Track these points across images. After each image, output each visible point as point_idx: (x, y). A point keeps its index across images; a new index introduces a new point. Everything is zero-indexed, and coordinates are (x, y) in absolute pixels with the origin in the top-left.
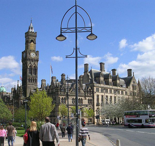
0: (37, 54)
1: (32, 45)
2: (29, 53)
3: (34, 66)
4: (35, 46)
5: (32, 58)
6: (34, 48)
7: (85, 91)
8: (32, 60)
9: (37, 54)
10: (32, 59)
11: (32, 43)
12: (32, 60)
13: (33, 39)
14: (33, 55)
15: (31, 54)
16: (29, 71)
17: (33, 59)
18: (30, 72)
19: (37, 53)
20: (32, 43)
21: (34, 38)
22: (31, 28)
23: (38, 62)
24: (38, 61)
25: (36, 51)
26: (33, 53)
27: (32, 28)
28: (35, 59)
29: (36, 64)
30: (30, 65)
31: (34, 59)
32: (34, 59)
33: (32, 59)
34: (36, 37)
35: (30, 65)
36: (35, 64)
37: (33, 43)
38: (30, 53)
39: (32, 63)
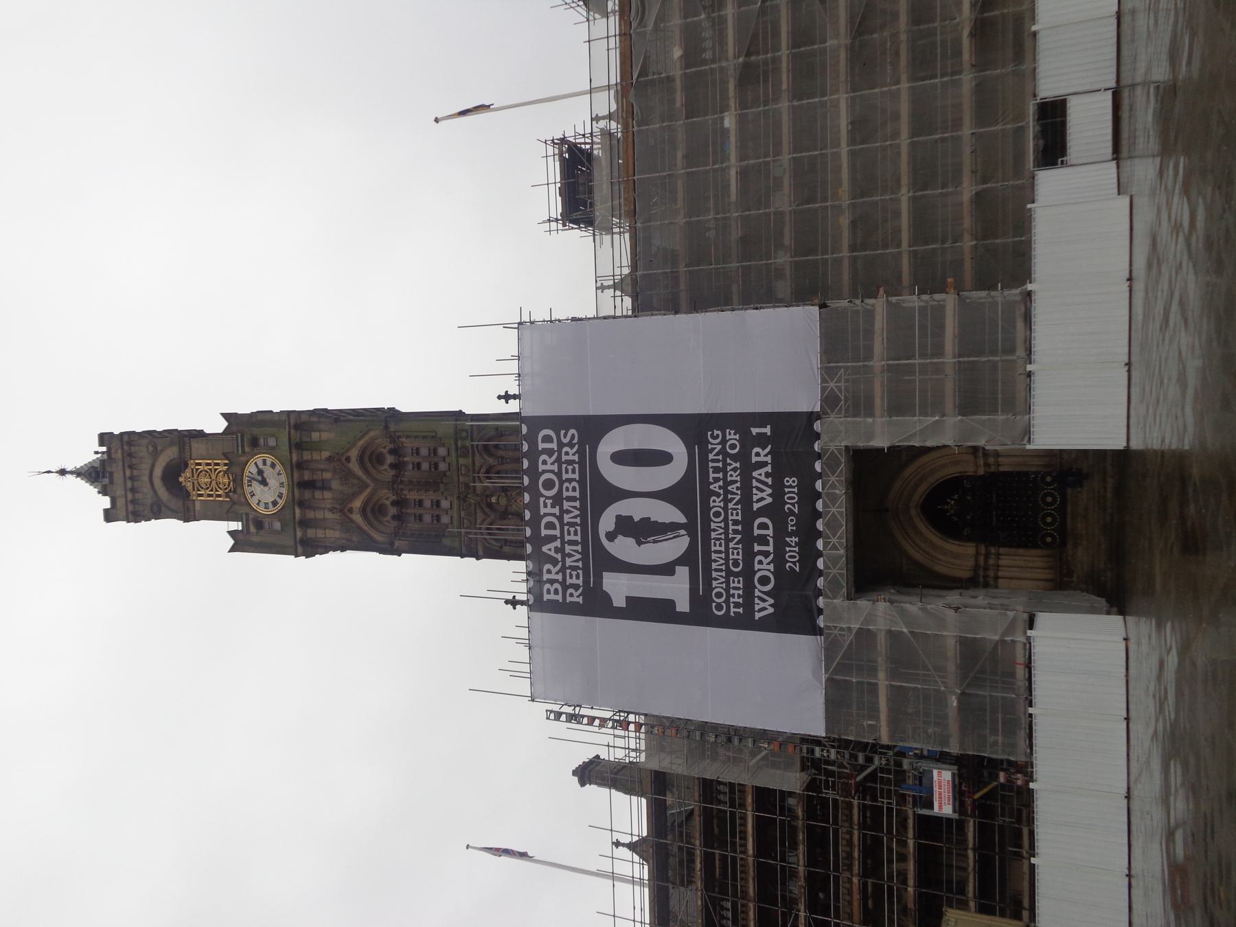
8: (304, 485)
11: (189, 486)
13: (158, 472)
15: (261, 510)
35: (357, 518)
37: (188, 473)
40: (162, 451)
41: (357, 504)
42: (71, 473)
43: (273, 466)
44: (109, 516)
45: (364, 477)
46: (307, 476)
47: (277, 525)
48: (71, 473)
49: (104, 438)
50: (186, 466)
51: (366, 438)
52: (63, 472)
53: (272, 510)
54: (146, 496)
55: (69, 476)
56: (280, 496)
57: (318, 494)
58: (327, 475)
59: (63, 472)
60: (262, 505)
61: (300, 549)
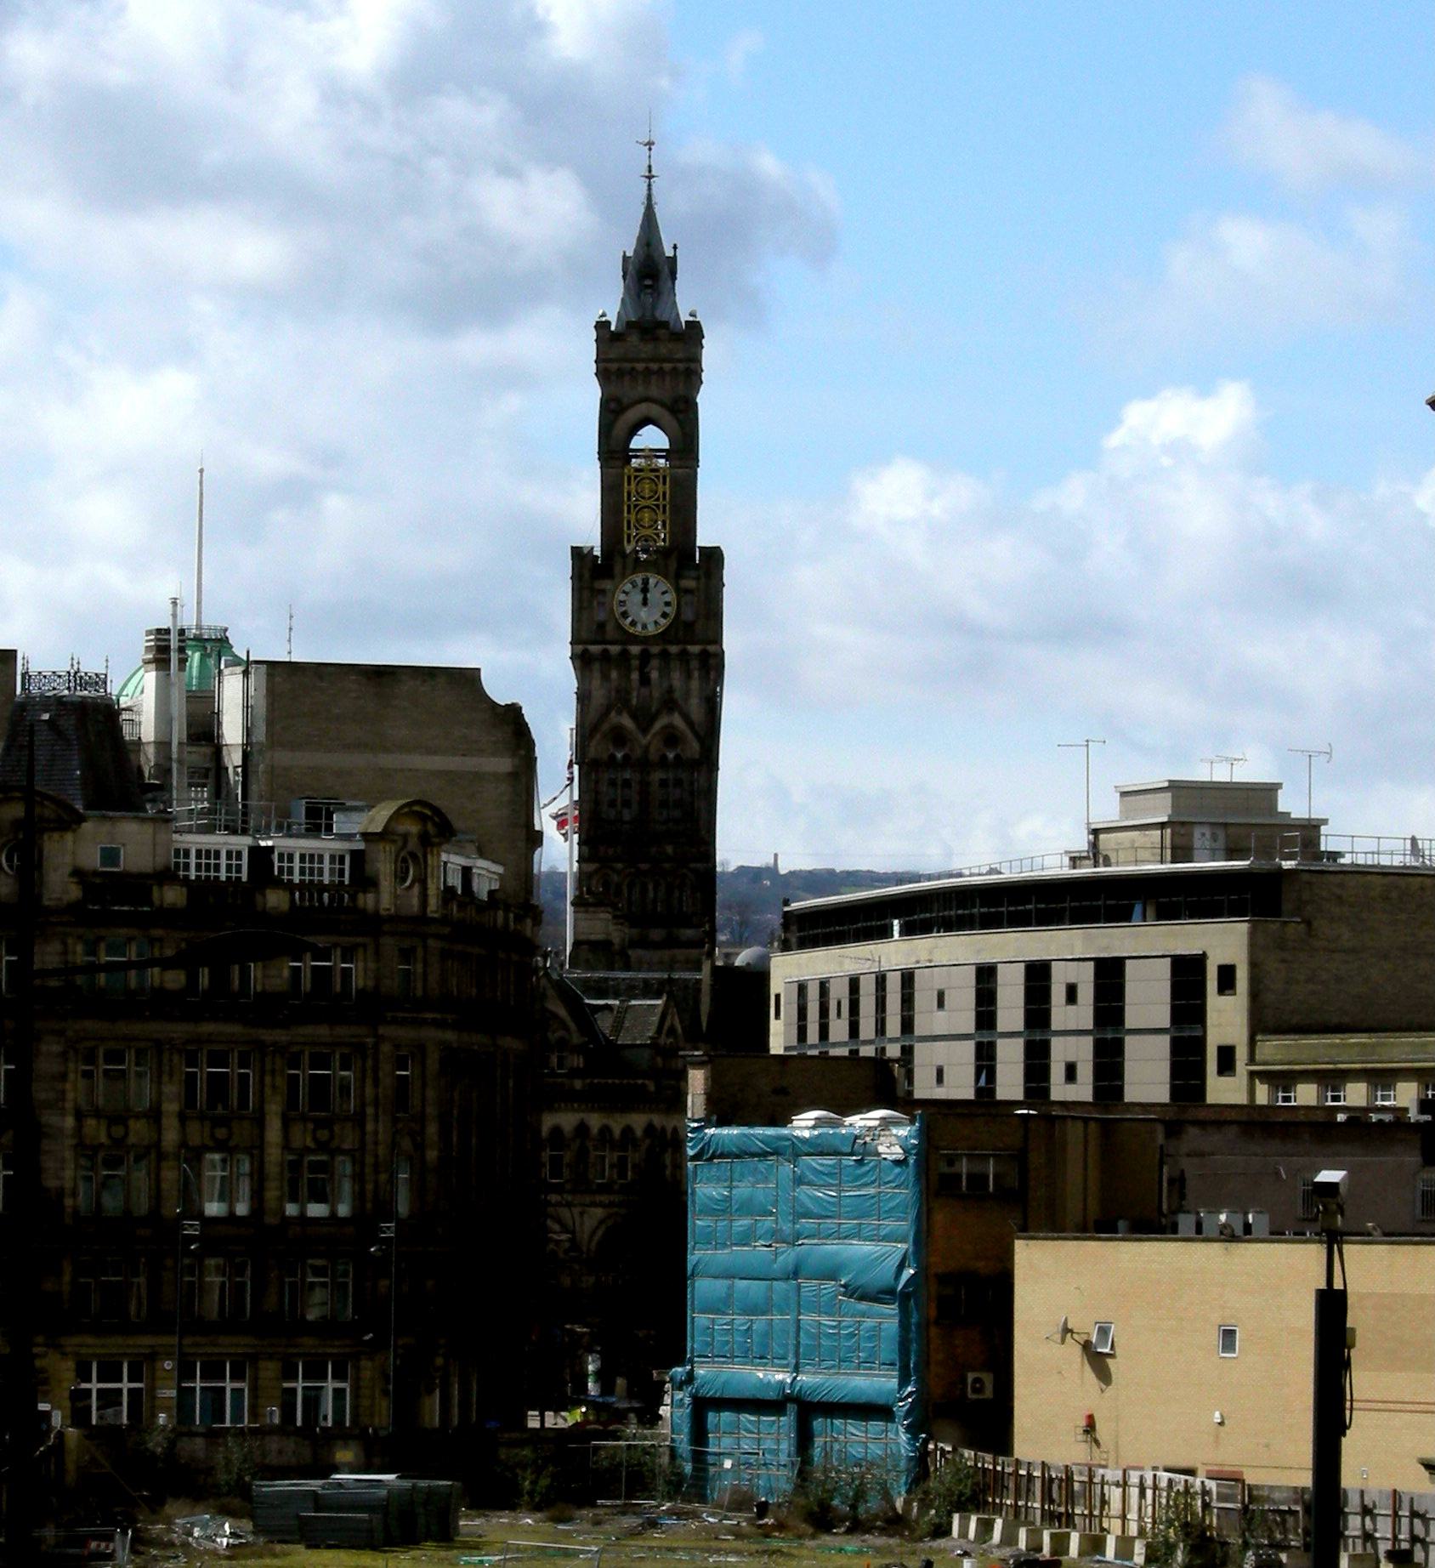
1: (647, 486)
3: (658, 726)
5: (635, 639)
12: (635, 663)
31: (655, 650)
32: (655, 650)
33: (635, 649)
40: (678, 420)
41: (627, 721)
42: (649, 197)
43: (664, 615)
44: (601, 326)
45: (653, 731)
46: (655, 663)
47: (601, 616)
48: (649, 197)
51: (690, 735)
53: (618, 610)
54: (629, 391)
57: (635, 676)
59: (650, 177)
60: (622, 597)
61: (580, 648)
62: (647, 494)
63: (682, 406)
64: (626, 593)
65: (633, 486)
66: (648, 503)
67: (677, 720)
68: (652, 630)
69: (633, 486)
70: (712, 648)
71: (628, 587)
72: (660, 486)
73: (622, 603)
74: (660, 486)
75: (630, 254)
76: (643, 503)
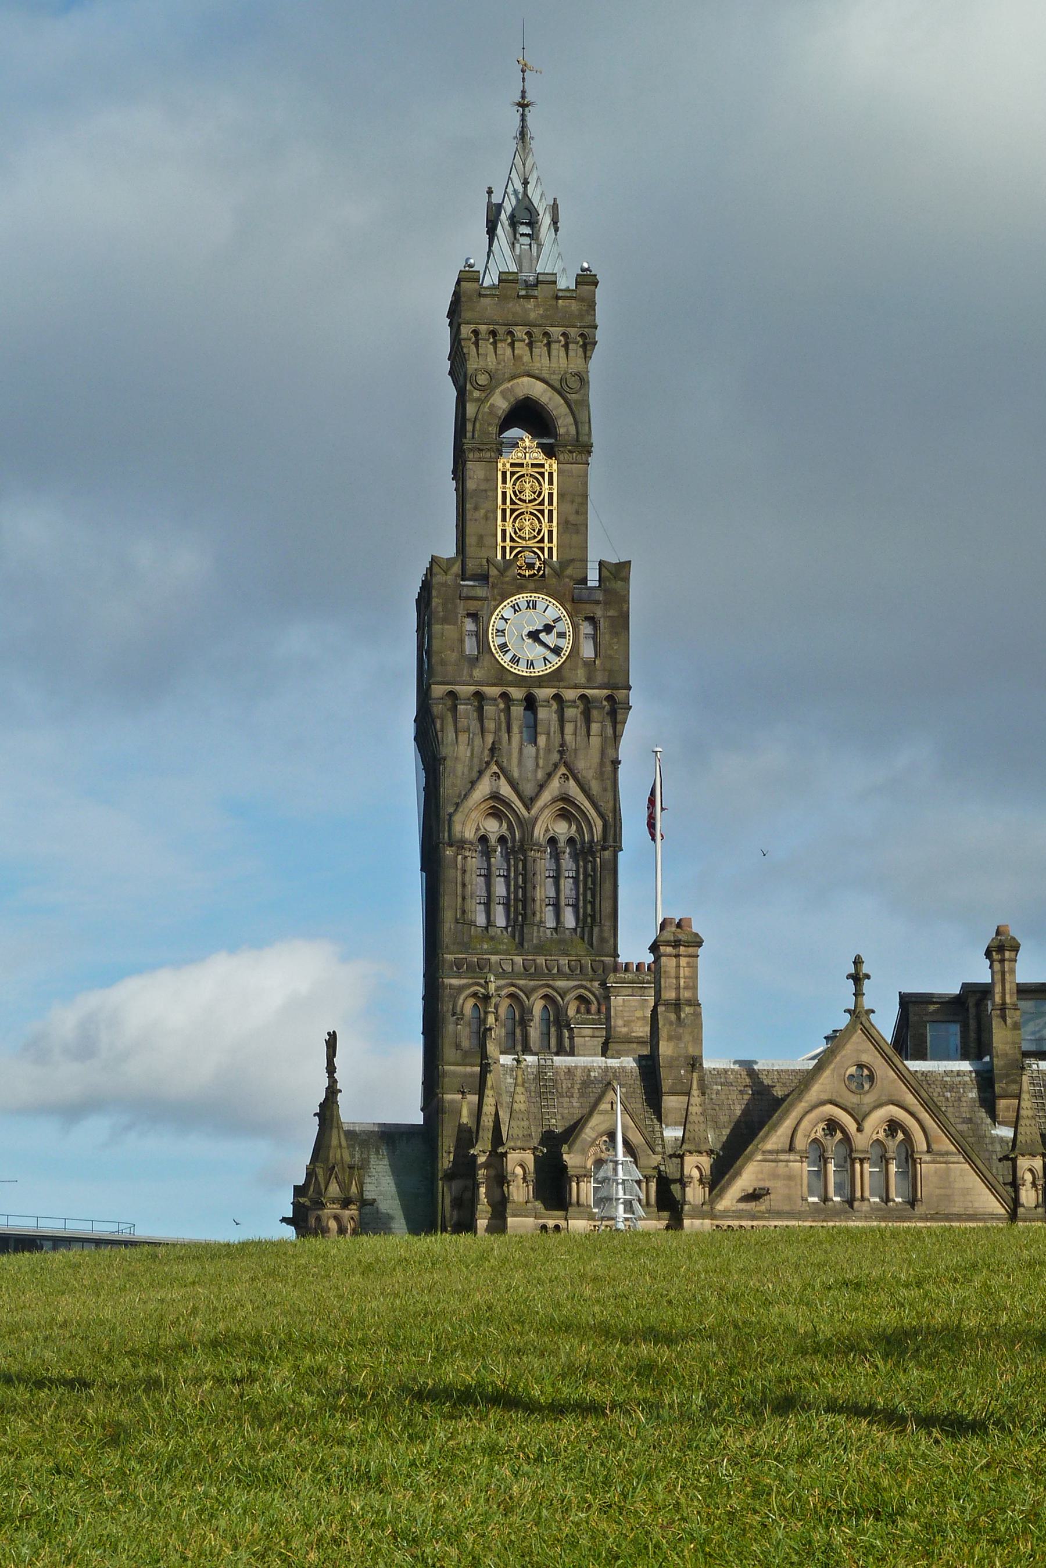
0: (599, 611)
2: (474, 616)
3: (546, 796)
4: (575, 498)
5: (521, 681)
6: (566, 525)
7: (1015, 1184)
9: (591, 620)
10: (517, 693)
11: (516, 456)
12: (517, 711)
13: (538, 390)
14: (525, 633)
15: (495, 623)
16: (488, 877)
17: (530, 703)
18: (500, 889)
19: (601, 601)
20: (526, 450)
21: (560, 362)
22: (514, 222)
23: (616, 737)
24: (616, 711)
25: (593, 577)
26: (532, 605)
27: (533, 223)
28: (570, 694)
29: (587, 764)
30: (484, 788)
31: (544, 693)
33: (517, 693)
34: (588, 344)
36: (572, 773)
37: (540, 457)
38: (473, 606)
39: (525, 758)
46: (542, 713)
49: (587, 280)
50: (549, 452)
52: (523, 106)
55: (518, 117)
56: (515, 660)
58: (542, 740)
59: (523, 106)
62: (528, 495)
63: (574, 383)
64: (506, 620)
65: (509, 484)
66: (532, 507)
67: (573, 789)
68: (540, 670)
69: (509, 484)
70: (620, 694)
71: (508, 613)
72: (546, 486)
73: (501, 632)
74: (546, 486)
75: (496, 199)
76: (522, 507)
